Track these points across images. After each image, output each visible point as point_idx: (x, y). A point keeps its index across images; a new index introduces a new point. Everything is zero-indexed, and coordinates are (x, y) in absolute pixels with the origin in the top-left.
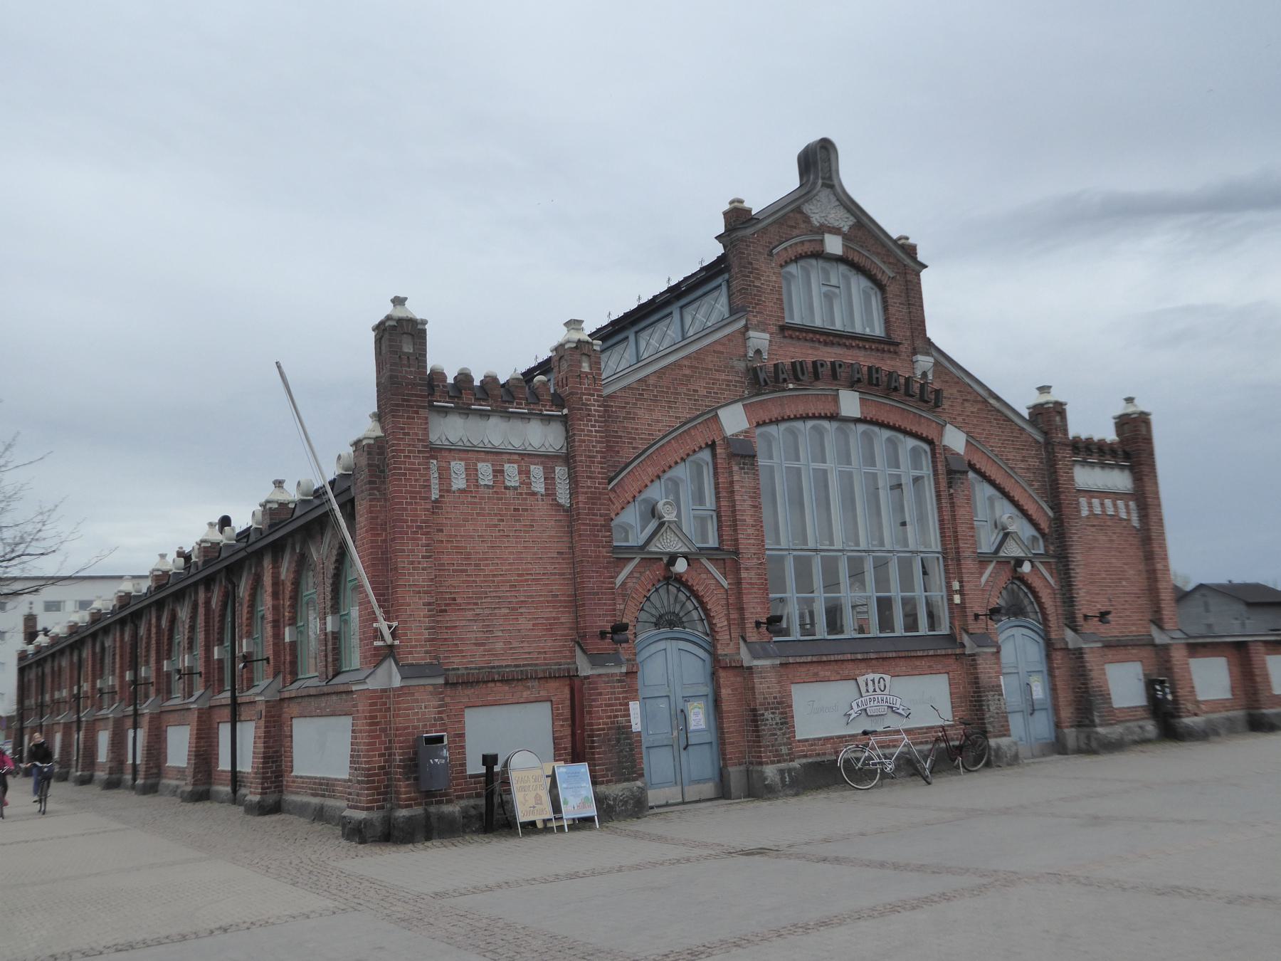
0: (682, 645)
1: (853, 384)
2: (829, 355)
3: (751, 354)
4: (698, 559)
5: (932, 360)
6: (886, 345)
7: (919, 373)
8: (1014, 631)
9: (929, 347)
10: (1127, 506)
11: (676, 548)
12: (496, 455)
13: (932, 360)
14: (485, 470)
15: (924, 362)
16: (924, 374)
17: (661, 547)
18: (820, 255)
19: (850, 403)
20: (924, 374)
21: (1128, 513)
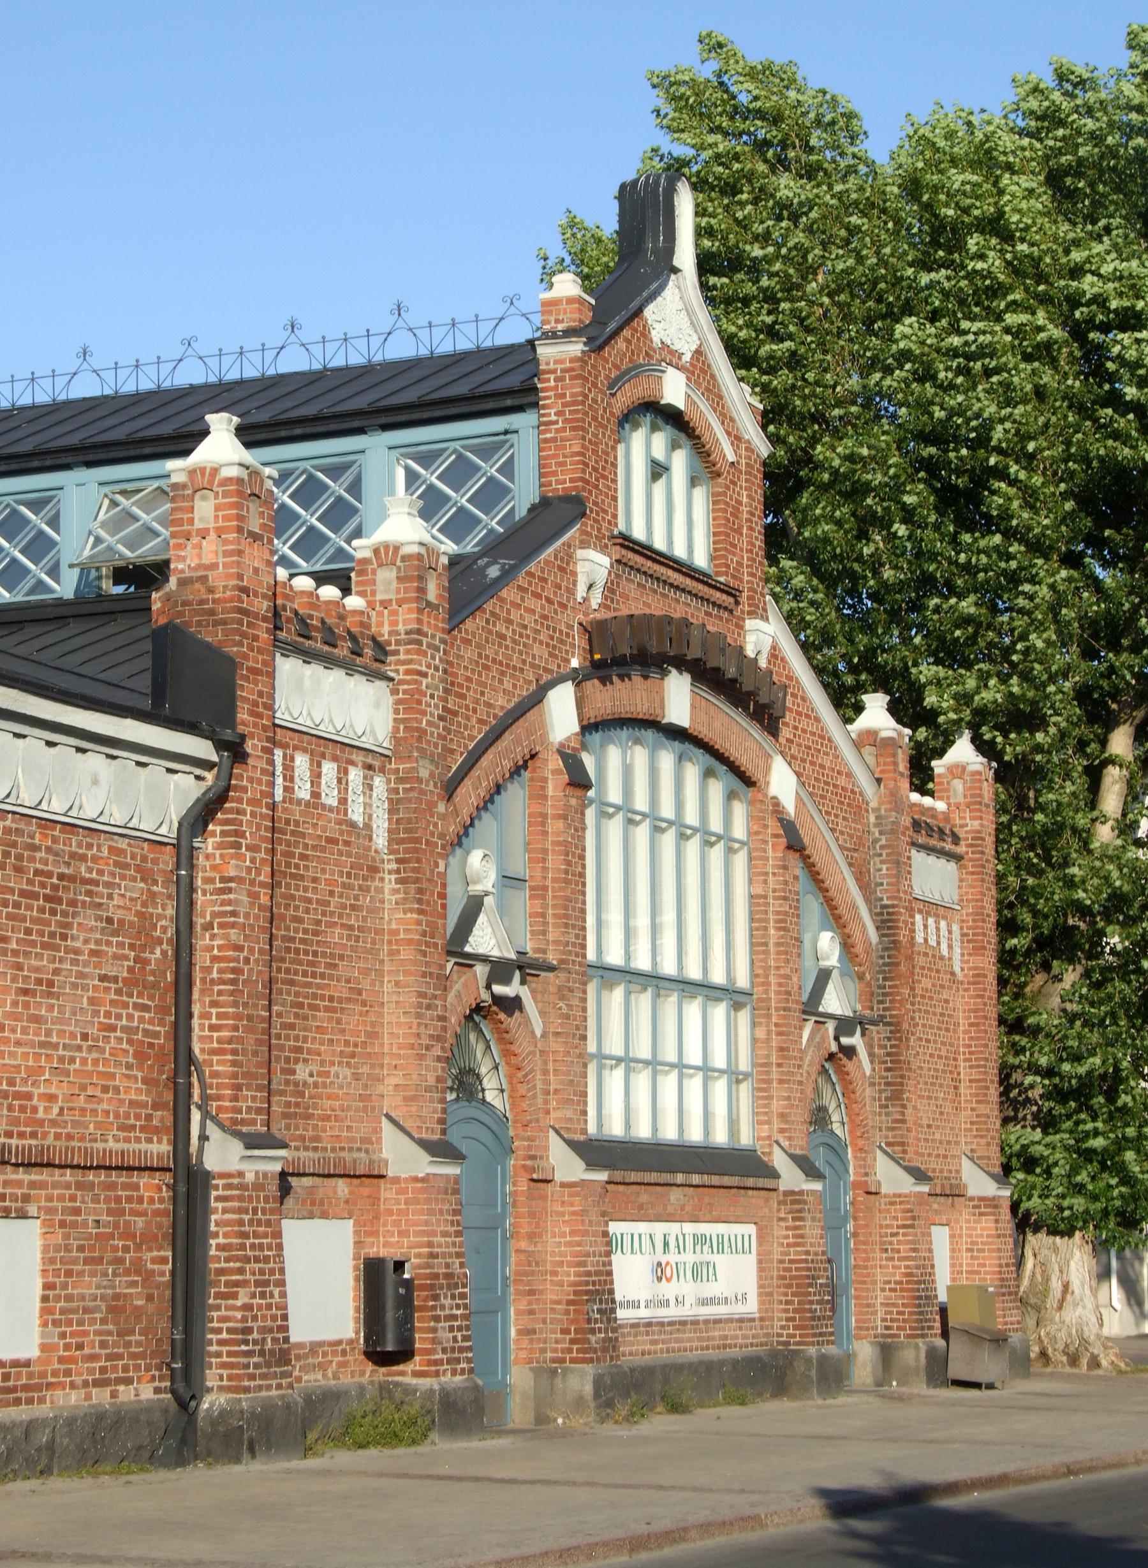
21: (950, 947)
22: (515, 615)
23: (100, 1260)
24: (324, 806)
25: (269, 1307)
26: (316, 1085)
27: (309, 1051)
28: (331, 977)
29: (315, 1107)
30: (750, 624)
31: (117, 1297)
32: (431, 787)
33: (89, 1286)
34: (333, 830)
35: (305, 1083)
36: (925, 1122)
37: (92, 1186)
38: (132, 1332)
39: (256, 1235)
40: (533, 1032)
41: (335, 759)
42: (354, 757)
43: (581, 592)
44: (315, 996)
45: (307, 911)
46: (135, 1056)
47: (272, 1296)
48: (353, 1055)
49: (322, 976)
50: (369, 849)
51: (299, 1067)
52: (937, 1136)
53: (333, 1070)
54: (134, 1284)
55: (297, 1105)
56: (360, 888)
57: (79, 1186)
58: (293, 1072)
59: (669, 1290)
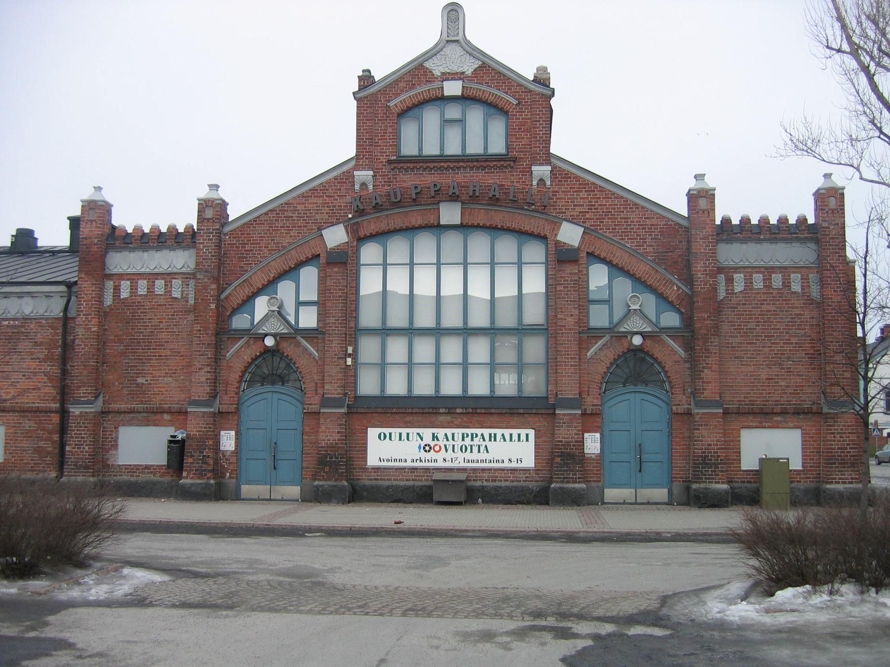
0: (281, 396)
1: (454, 198)
2: (428, 179)
3: (357, 187)
4: (295, 338)
5: (549, 168)
6: (503, 161)
7: (535, 183)
8: (631, 396)
9: (547, 157)
10: (805, 279)
11: (642, 328)
12: (152, 277)
13: (549, 168)
14: (160, 284)
15: (541, 171)
16: (541, 180)
17: (266, 330)
18: (441, 99)
19: (450, 214)
20: (541, 180)
22: (300, 207)
23: (31, 437)
24: (157, 295)
25: (83, 452)
26: (149, 384)
27: (145, 373)
28: (161, 349)
29: (149, 391)
30: (533, 168)
31: (40, 447)
32: (206, 280)
33: (25, 444)
34: (162, 302)
35: (143, 384)
36: (764, 376)
37: (28, 416)
38: (47, 457)
39: (77, 430)
40: (314, 358)
41: (163, 279)
42: (176, 277)
43: (357, 187)
44: (150, 356)
45: (145, 329)
46: (48, 379)
47: (84, 448)
48: (175, 373)
49: (153, 349)
50: (187, 305)
51: (138, 379)
52: (783, 384)
53: (160, 378)
54: (48, 444)
55: (139, 391)
56: (180, 318)
57: (20, 416)
58: (136, 380)
59: (429, 456)
